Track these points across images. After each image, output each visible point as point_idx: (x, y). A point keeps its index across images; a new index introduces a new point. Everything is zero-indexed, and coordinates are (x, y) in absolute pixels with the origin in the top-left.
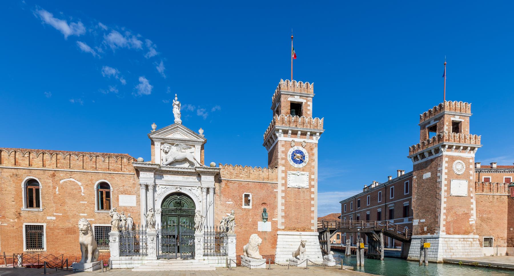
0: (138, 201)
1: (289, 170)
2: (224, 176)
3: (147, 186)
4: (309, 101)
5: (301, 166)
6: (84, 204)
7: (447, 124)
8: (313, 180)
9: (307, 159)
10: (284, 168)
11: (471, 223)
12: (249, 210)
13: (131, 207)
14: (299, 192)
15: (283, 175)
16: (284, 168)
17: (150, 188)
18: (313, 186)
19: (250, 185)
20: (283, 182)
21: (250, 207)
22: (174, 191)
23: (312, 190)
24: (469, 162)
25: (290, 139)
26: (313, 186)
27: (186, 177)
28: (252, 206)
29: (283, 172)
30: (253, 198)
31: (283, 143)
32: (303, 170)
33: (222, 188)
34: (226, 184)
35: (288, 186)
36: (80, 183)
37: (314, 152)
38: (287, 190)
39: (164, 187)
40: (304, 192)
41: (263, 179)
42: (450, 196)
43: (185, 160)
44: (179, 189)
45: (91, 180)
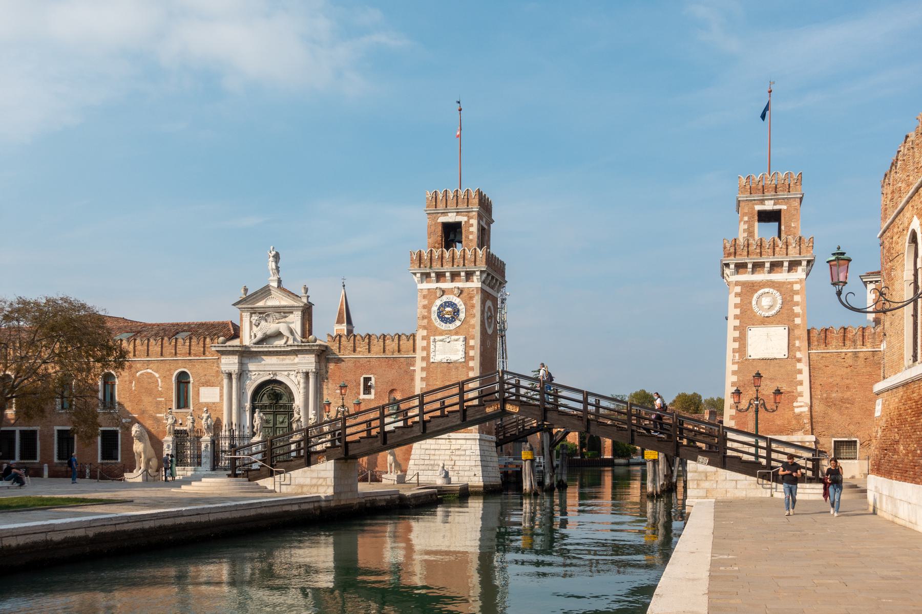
0: (221, 396)
1: (434, 335)
3: (230, 375)
4: (472, 218)
5: (452, 326)
7: (746, 219)
8: (473, 348)
9: (462, 315)
10: (425, 333)
11: (797, 411)
13: (214, 403)
14: (449, 369)
15: (424, 343)
16: (425, 333)
17: (234, 377)
18: (472, 358)
19: (372, 363)
20: (424, 354)
21: (372, 396)
22: (267, 378)
23: (471, 364)
24: (792, 290)
25: (434, 285)
26: (472, 358)
29: (423, 338)
30: (376, 382)
31: (425, 292)
32: (457, 333)
35: (432, 360)
36: (157, 375)
37: (474, 302)
38: (430, 367)
40: (457, 368)
41: (393, 353)
42: (744, 362)
43: (279, 335)
45: (170, 370)
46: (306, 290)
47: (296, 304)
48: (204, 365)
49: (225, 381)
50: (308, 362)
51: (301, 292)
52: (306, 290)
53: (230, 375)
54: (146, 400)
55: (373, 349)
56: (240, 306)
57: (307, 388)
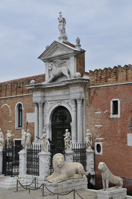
2: (92, 83)
6: (10, 123)
12: (117, 119)
17: (39, 105)
21: (119, 116)
22: (57, 105)
27: (64, 90)
28: (121, 114)
33: (91, 97)
34: (94, 92)
39: (50, 103)
44: (59, 104)
46: (78, 41)
47: (70, 52)
48: (29, 99)
49: (36, 108)
50: (77, 92)
51: (75, 43)
52: (78, 41)
53: (37, 104)
54: (5, 121)
55: (120, 78)
56: (42, 58)
57: (76, 111)
